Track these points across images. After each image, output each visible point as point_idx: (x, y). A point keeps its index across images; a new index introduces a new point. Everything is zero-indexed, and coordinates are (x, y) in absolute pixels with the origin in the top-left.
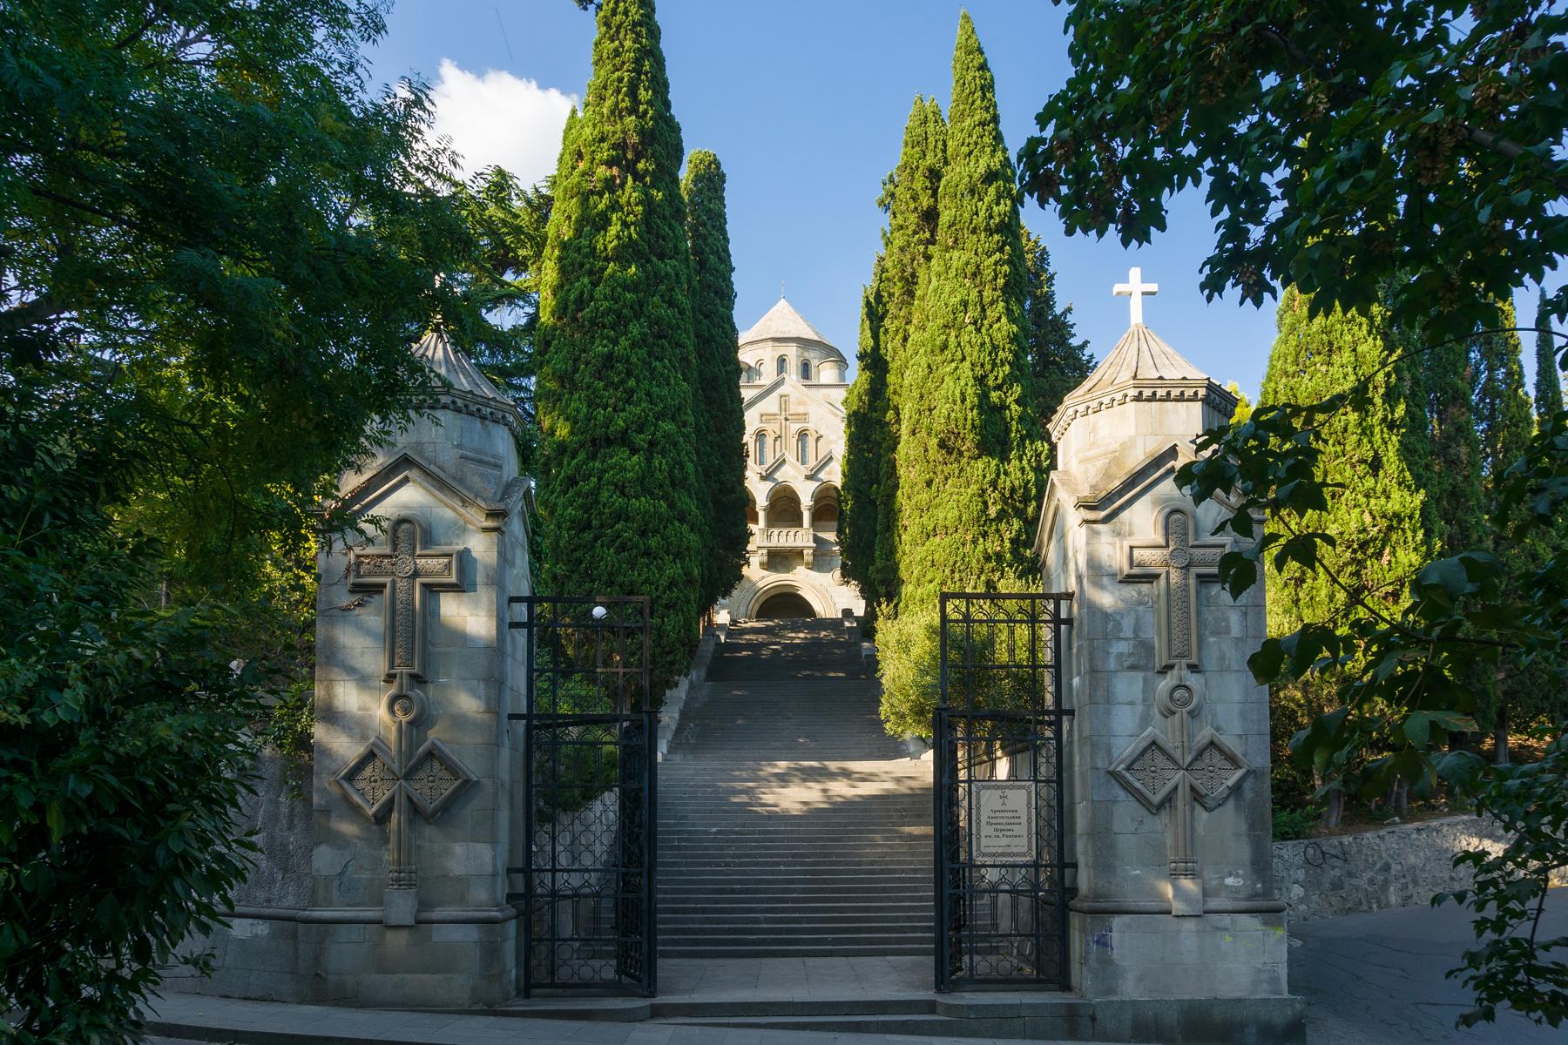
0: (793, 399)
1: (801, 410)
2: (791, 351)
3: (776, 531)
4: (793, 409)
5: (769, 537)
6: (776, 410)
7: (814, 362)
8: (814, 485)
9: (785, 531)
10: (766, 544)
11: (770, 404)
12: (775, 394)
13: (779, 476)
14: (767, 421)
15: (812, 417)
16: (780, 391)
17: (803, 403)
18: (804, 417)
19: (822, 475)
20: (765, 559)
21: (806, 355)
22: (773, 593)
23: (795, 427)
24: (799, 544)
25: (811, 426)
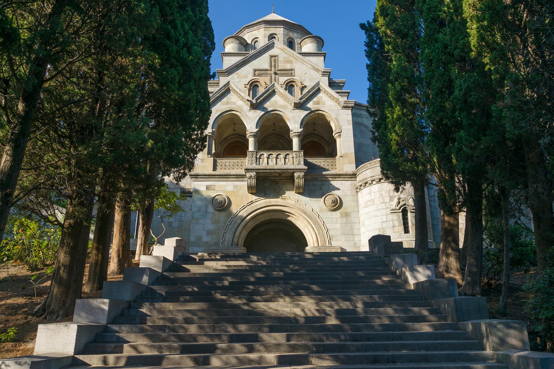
0: (281, 58)
1: (288, 66)
2: (280, 31)
3: (266, 155)
4: (281, 66)
5: (258, 160)
6: (267, 66)
7: (297, 41)
8: (303, 114)
9: (274, 154)
10: (254, 166)
11: (262, 62)
12: (266, 56)
13: (269, 105)
14: (259, 75)
15: (297, 72)
16: (272, 52)
17: (290, 62)
18: (290, 72)
19: (310, 105)
20: (254, 182)
21: (291, 35)
22: (262, 219)
23: (283, 79)
24: (290, 165)
25: (296, 78)
